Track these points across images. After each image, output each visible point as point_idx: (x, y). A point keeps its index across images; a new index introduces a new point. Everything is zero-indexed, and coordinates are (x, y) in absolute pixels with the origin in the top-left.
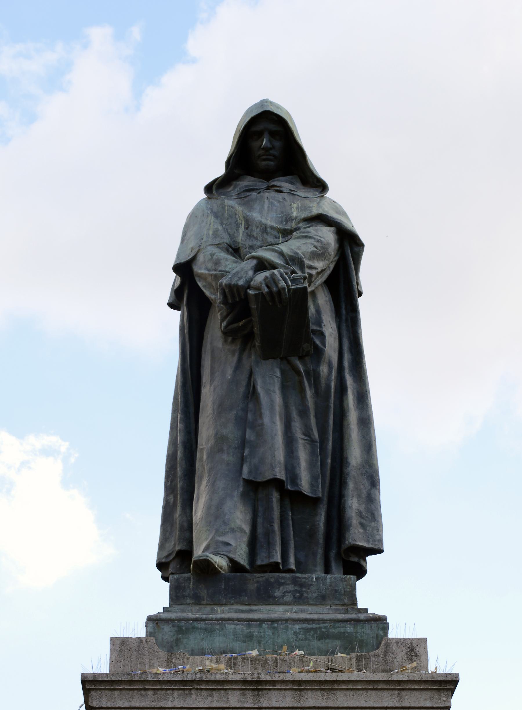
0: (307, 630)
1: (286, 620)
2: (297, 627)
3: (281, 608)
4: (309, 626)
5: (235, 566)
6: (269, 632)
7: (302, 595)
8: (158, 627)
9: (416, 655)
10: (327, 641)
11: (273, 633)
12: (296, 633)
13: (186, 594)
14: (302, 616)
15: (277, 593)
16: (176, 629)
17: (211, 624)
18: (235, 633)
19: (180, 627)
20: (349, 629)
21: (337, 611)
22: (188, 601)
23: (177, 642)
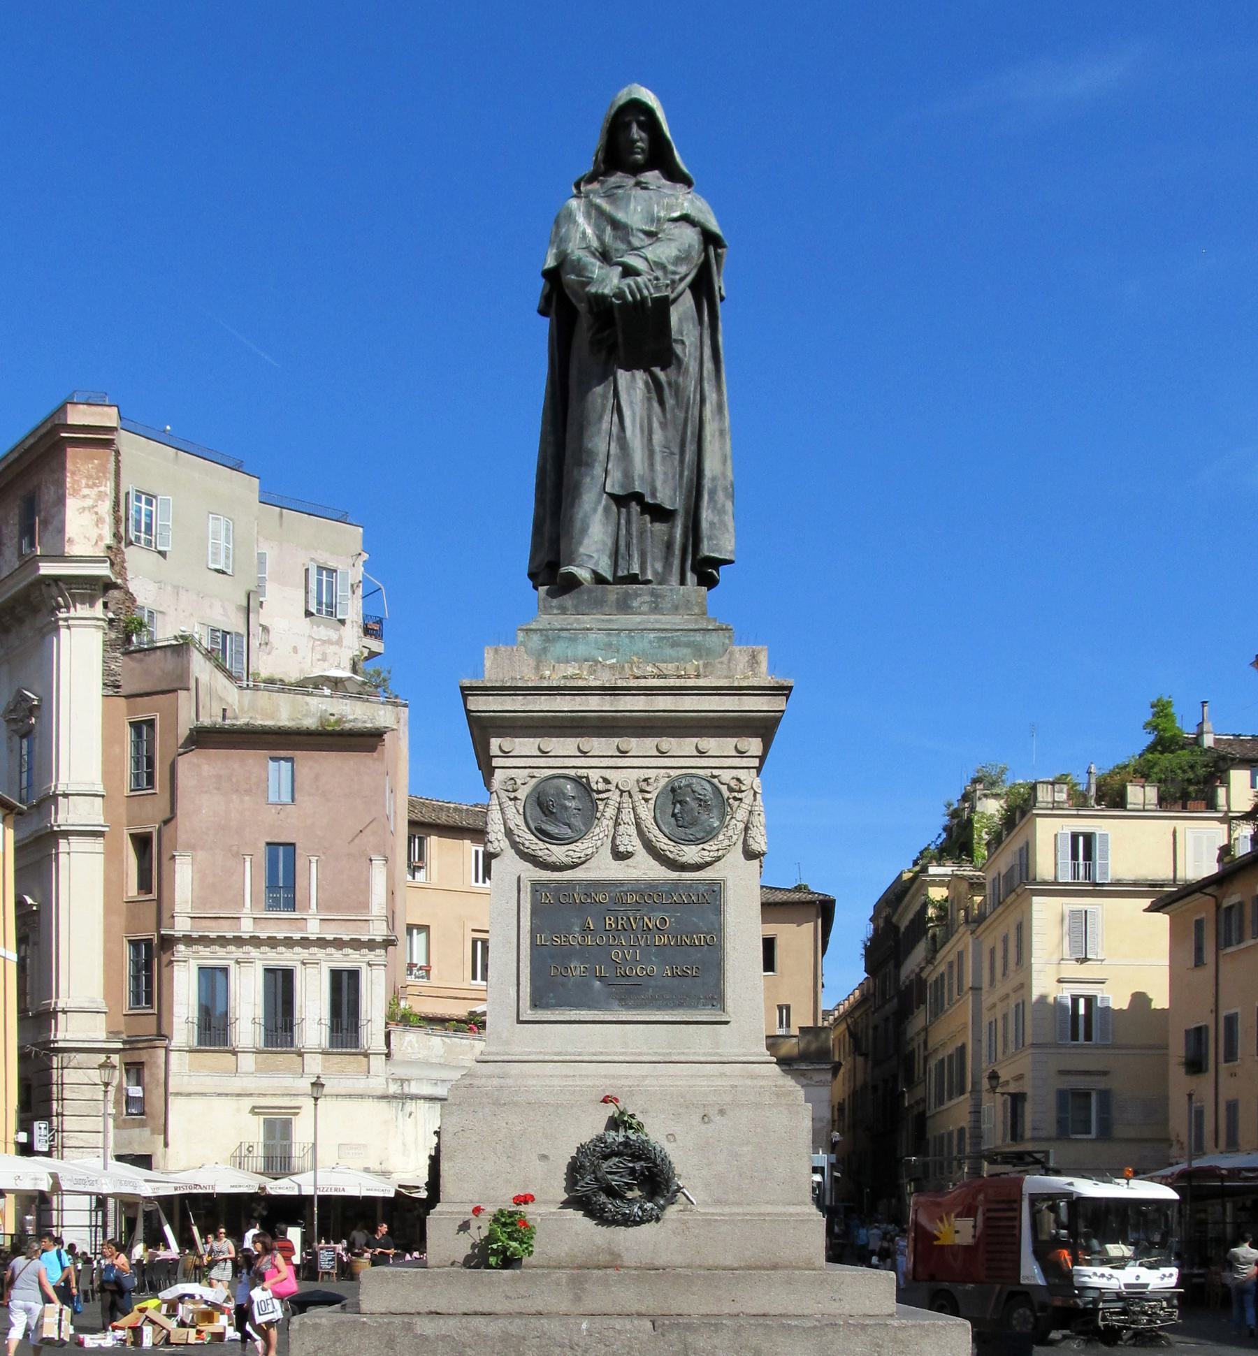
0: (661, 639)
1: (642, 630)
2: (652, 635)
3: (638, 618)
4: (662, 635)
5: (599, 579)
6: (626, 641)
7: (657, 606)
8: (528, 636)
9: (757, 663)
10: (679, 649)
11: (631, 642)
12: (650, 642)
13: (553, 604)
14: (658, 626)
15: (635, 604)
16: (543, 638)
17: (574, 634)
18: (596, 642)
19: (547, 636)
20: (698, 637)
21: (688, 621)
22: (555, 611)
23: (545, 650)
